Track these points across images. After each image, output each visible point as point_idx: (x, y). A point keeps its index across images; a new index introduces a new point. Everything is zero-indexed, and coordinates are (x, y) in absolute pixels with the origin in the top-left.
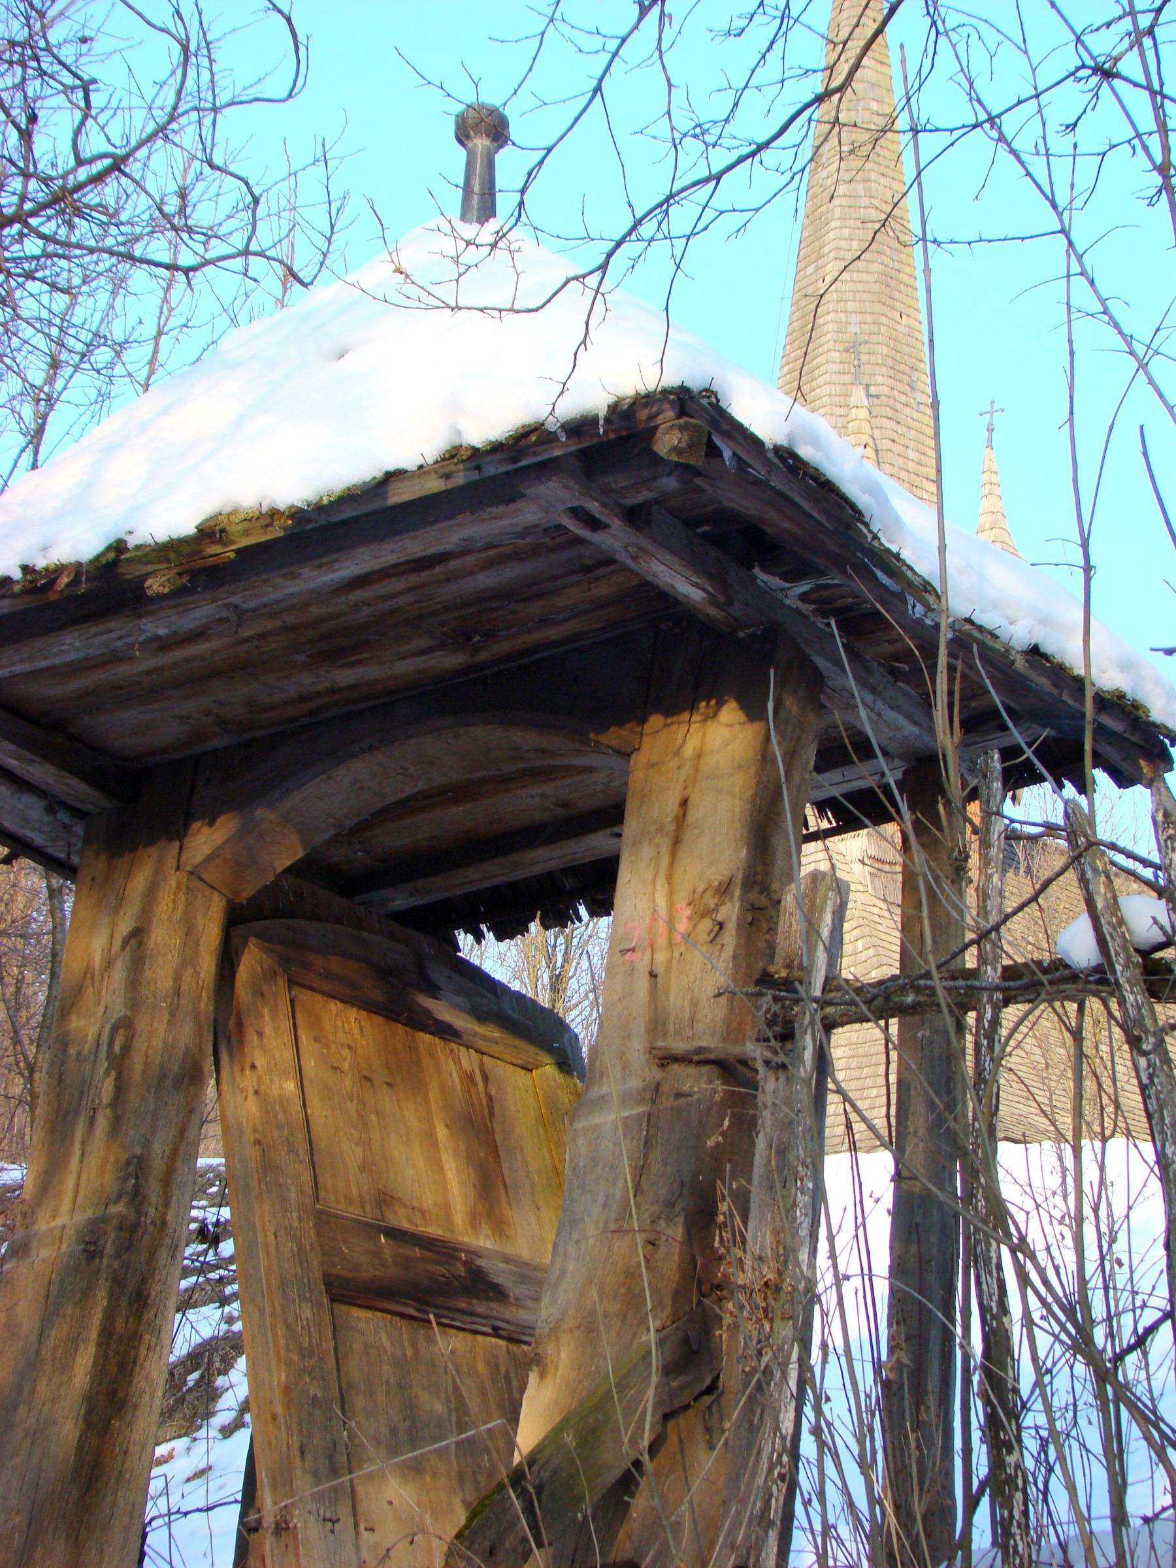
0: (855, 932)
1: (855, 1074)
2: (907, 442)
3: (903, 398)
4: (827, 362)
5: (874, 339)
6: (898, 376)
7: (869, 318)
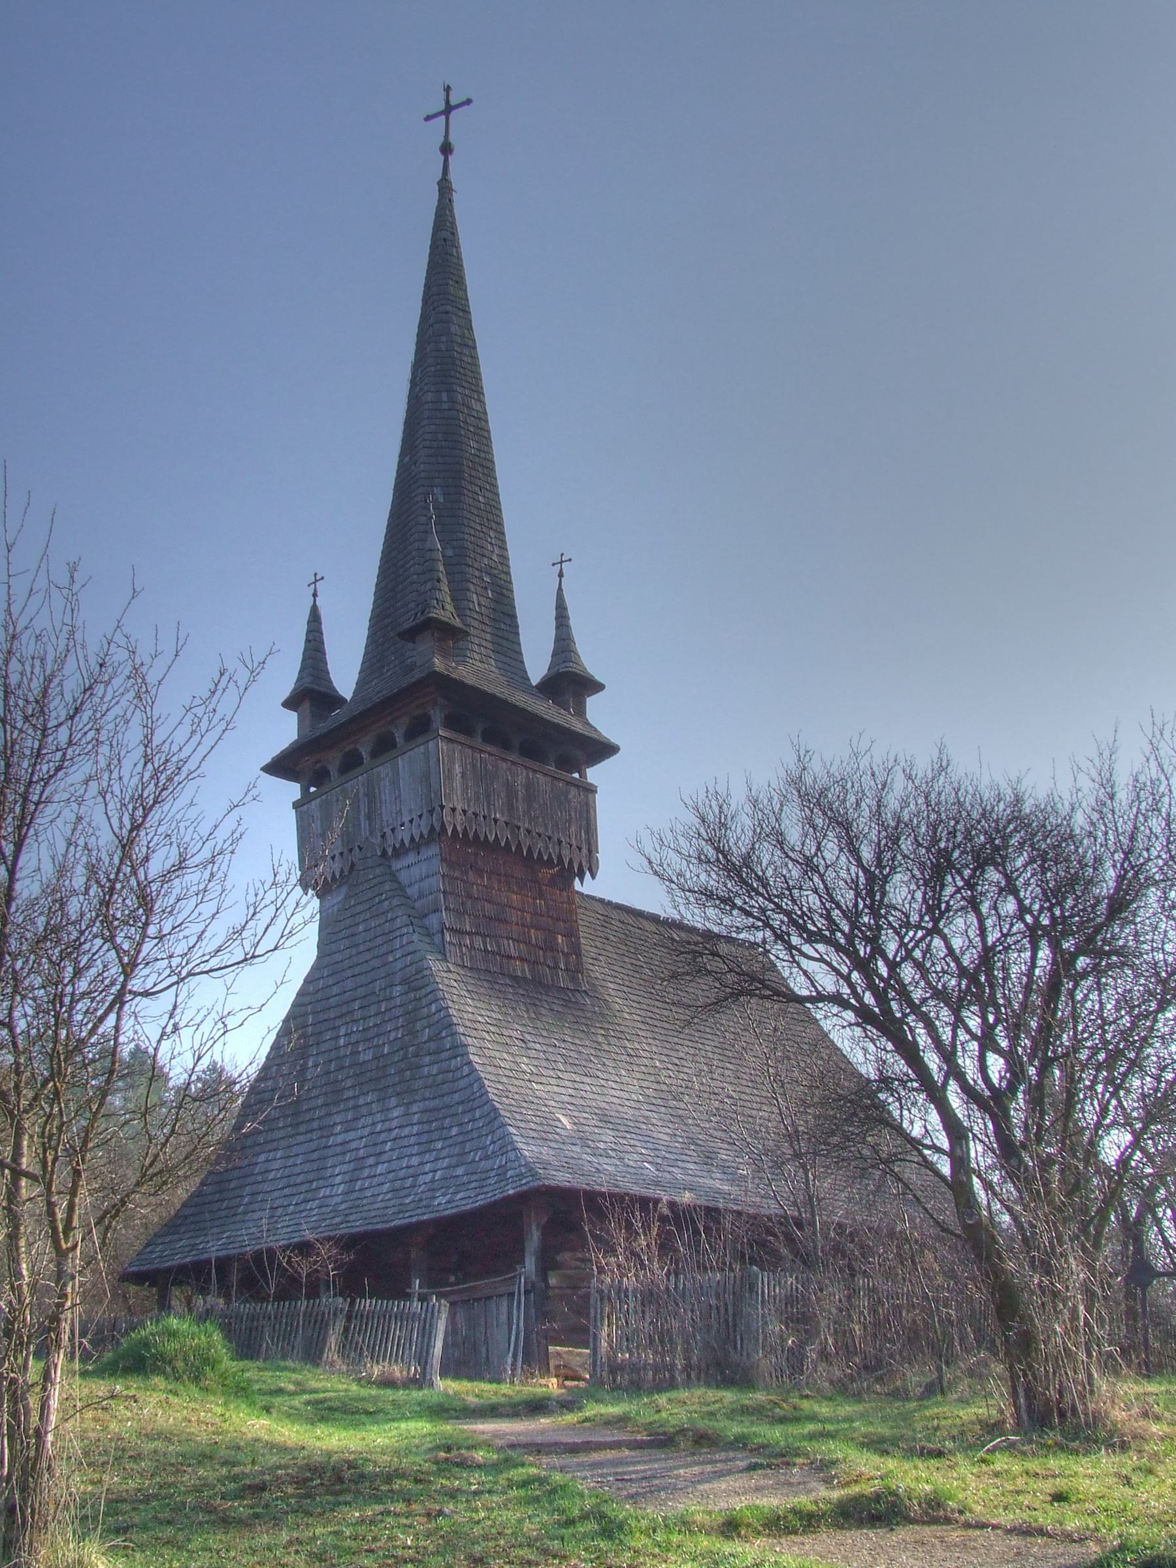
1: (426, 1127)
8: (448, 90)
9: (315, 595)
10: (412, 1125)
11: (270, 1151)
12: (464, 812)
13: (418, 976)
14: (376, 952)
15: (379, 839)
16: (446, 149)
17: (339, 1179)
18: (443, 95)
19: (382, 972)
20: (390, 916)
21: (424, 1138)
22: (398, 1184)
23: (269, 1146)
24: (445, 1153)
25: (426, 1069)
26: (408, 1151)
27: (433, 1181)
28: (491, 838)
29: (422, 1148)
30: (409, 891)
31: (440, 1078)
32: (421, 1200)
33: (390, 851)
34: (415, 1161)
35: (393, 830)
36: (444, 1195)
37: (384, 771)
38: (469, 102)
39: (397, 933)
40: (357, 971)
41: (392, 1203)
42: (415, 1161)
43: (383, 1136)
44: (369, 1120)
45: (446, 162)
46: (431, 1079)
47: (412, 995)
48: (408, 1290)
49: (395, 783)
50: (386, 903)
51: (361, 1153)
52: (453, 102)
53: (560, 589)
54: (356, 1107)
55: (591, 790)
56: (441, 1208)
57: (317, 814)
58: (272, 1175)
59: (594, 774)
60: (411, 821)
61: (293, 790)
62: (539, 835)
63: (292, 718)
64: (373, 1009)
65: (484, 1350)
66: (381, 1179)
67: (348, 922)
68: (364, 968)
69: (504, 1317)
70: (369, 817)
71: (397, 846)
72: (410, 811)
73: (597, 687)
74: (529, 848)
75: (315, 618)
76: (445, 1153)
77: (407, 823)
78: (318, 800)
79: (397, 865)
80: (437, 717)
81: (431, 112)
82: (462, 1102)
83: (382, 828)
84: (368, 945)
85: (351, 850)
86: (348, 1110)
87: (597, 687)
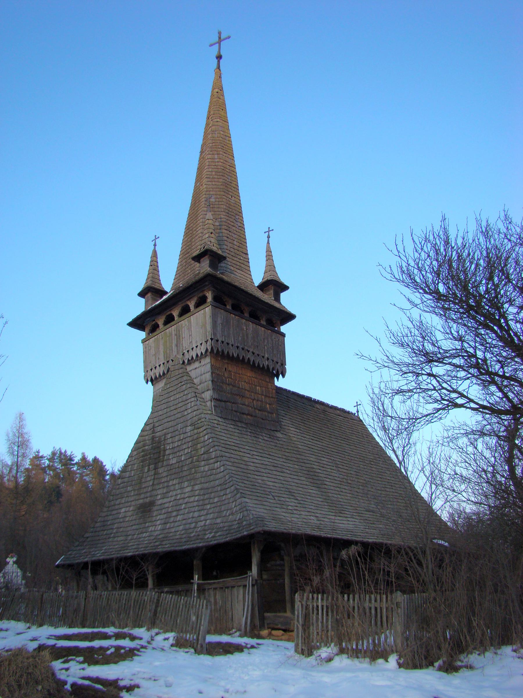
0: (204, 432)
1: (202, 498)
2: (234, 239)
3: (232, 224)
5: (220, 203)
6: (230, 216)
7: (218, 196)
8: (220, 33)
9: (155, 245)
10: (195, 496)
11: (127, 507)
12: (223, 342)
13: (199, 422)
14: (179, 410)
15: (182, 355)
16: (219, 57)
17: (159, 522)
18: (217, 35)
19: (182, 420)
20: (186, 392)
21: (201, 503)
22: (187, 526)
23: (127, 504)
24: (211, 511)
25: (202, 468)
26: (193, 509)
27: (205, 525)
28: (235, 355)
29: (200, 508)
30: (195, 381)
31: (209, 473)
32: (199, 535)
33: (186, 361)
34: (196, 514)
35: (188, 351)
36: (210, 533)
37: (184, 323)
38: (229, 37)
39: (189, 401)
40: (169, 419)
41: (184, 536)
42: (196, 514)
43: (181, 501)
44: (174, 493)
46: (204, 473)
47: (196, 431)
48: (192, 581)
49: (189, 329)
50: (184, 386)
51: (170, 510)
53: (268, 243)
54: (168, 486)
55: (283, 335)
56: (209, 540)
57: (153, 345)
58: (127, 519)
59: (284, 329)
60: (197, 347)
61: (142, 335)
62: (258, 355)
63: (143, 300)
64: (177, 438)
65: (230, 613)
66: (179, 523)
67: (166, 396)
68: (173, 418)
69: (241, 597)
70: (177, 346)
71: (190, 359)
72: (196, 342)
73: (285, 288)
74: (254, 361)
75: (155, 254)
76: (211, 511)
77: (195, 348)
78: (153, 338)
79: (189, 368)
80: (209, 296)
82: (220, 485)
83: (183, 350)
84: (175, 407)
85: (168, 362)
86: (164, 488)
87: (285, 288)
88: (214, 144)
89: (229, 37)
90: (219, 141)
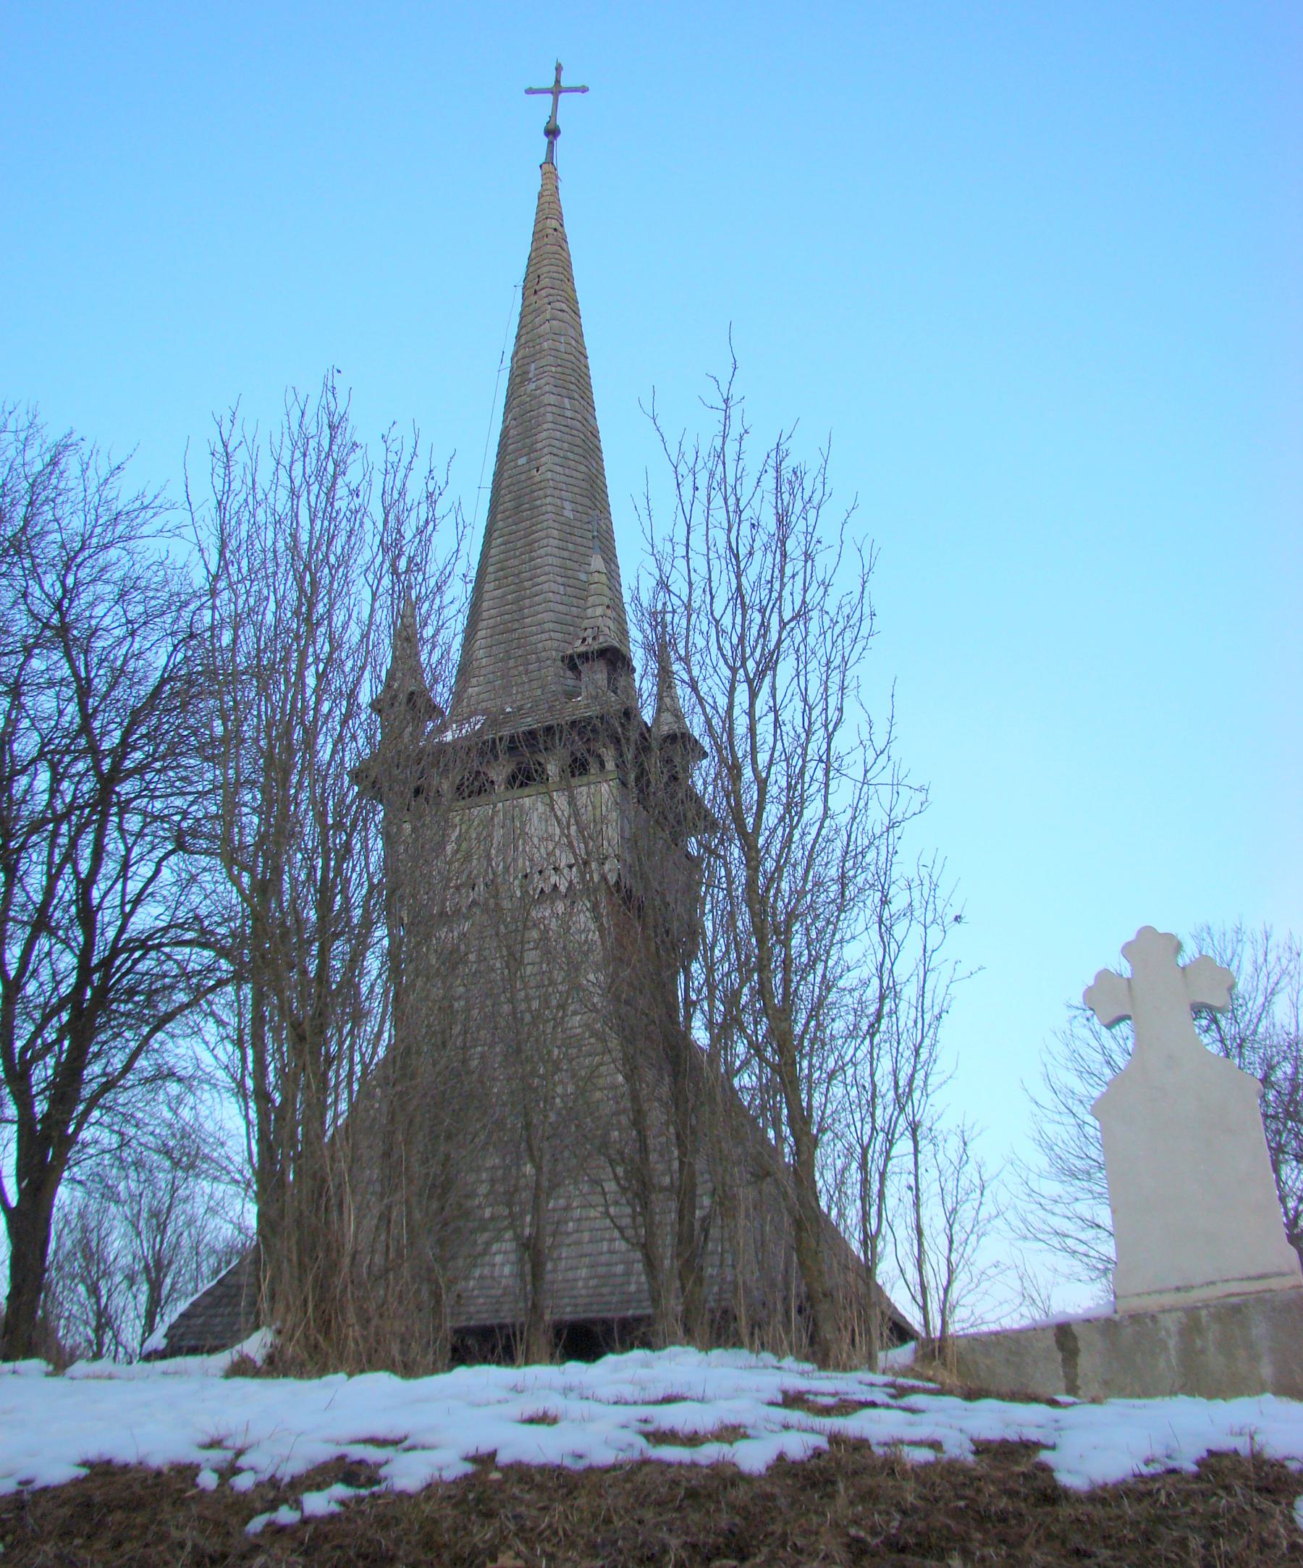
4: (548, 537)
8: (559, 69)
16: (552, 132)
45: (551, 144)
52: (564, 84)
81: (535, 87)
88: (559, 369)
89: (584, 90)
90: (569, 365)
